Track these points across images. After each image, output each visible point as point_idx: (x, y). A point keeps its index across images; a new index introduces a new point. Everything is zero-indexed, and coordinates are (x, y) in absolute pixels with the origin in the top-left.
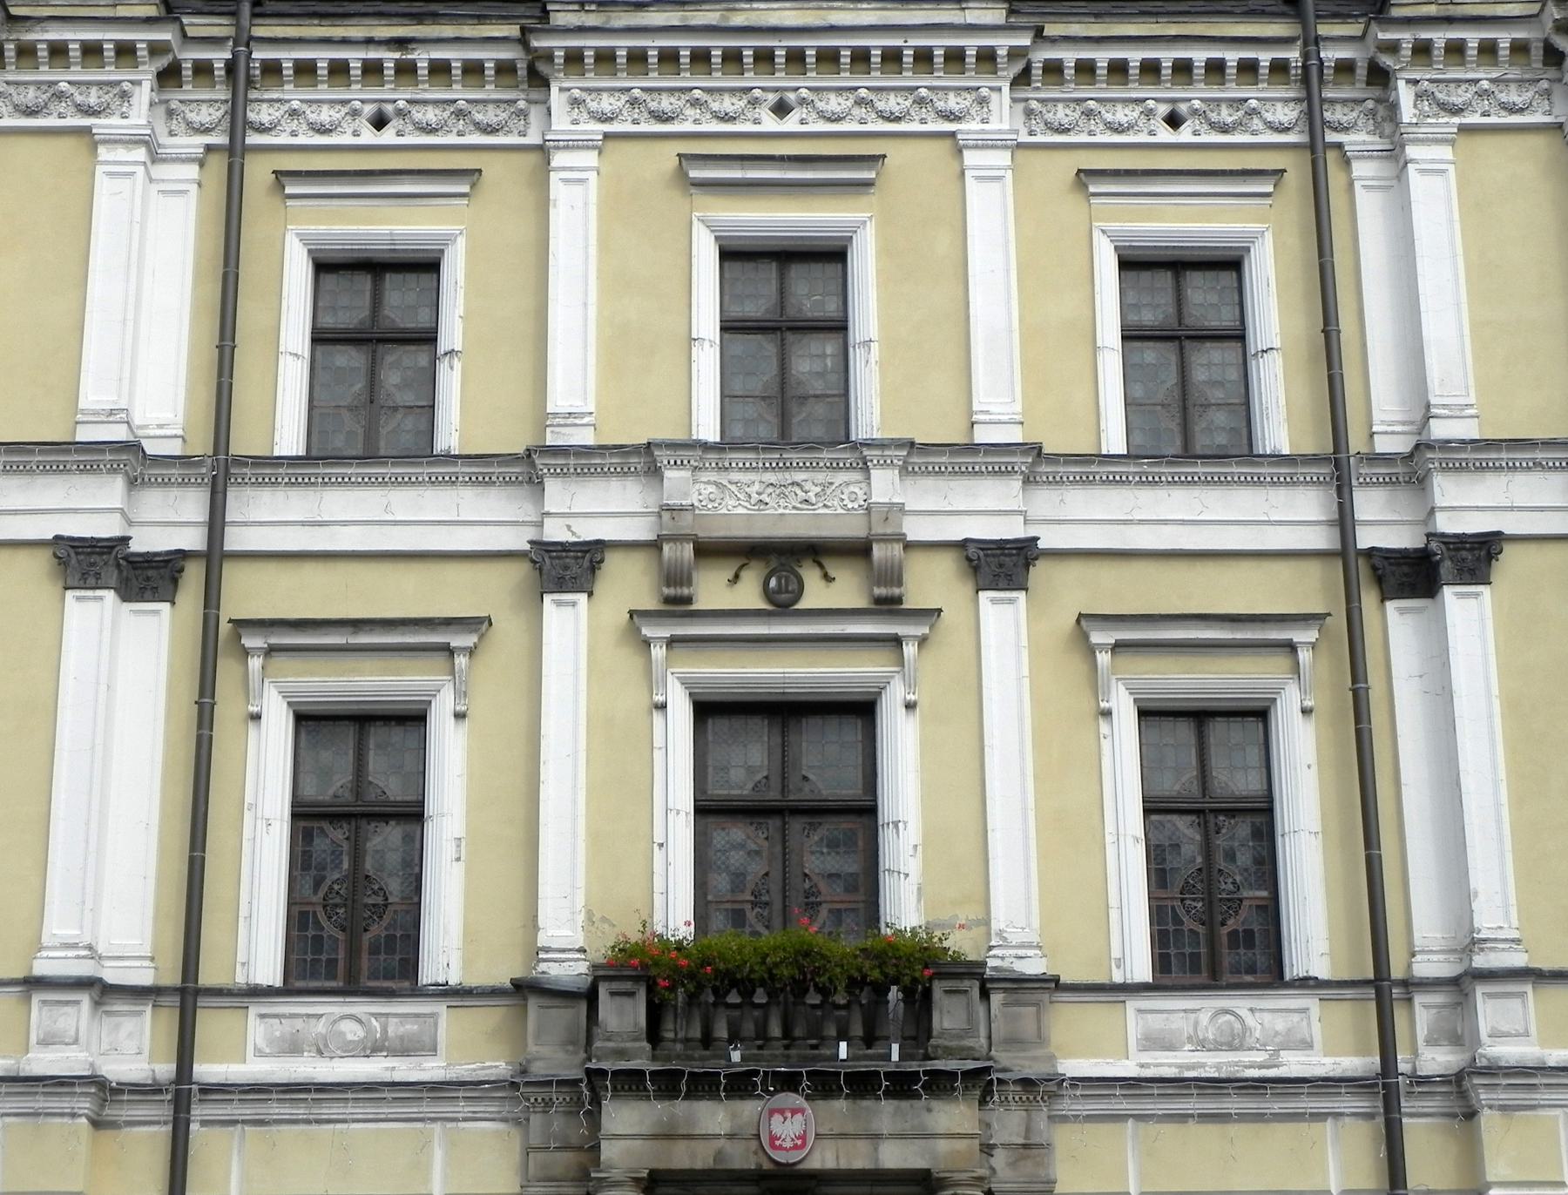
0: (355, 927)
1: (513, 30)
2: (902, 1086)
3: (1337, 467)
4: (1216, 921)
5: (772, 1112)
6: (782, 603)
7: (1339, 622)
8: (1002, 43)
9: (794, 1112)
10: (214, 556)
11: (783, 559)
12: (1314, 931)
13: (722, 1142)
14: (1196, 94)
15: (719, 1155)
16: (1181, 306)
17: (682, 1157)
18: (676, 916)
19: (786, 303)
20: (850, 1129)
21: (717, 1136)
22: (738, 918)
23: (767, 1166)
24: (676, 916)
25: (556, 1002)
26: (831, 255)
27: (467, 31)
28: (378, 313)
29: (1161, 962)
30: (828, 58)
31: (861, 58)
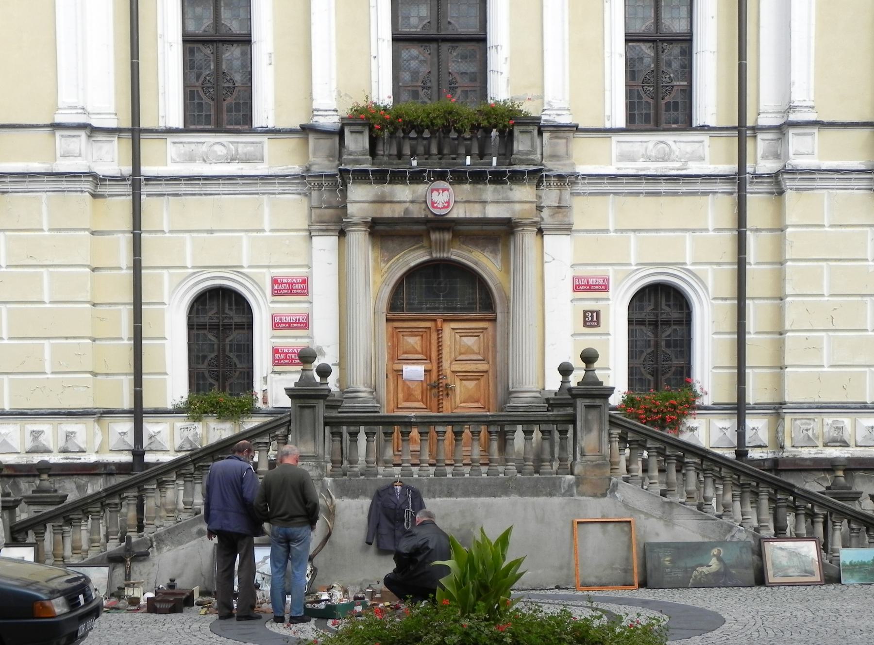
2: (498, 178)
4: (659, 94)
5: (432, 191)
9: (444, 190)
12: (710, 100)
13: (407, 205)
15: (406, 211)
17: (387, 212)
18: (383, 94)
20: (472, 198)
21: (405, 202)
22: (415, 95)
23: (430, 216)
24: (383, 94)
25: (323, 136)
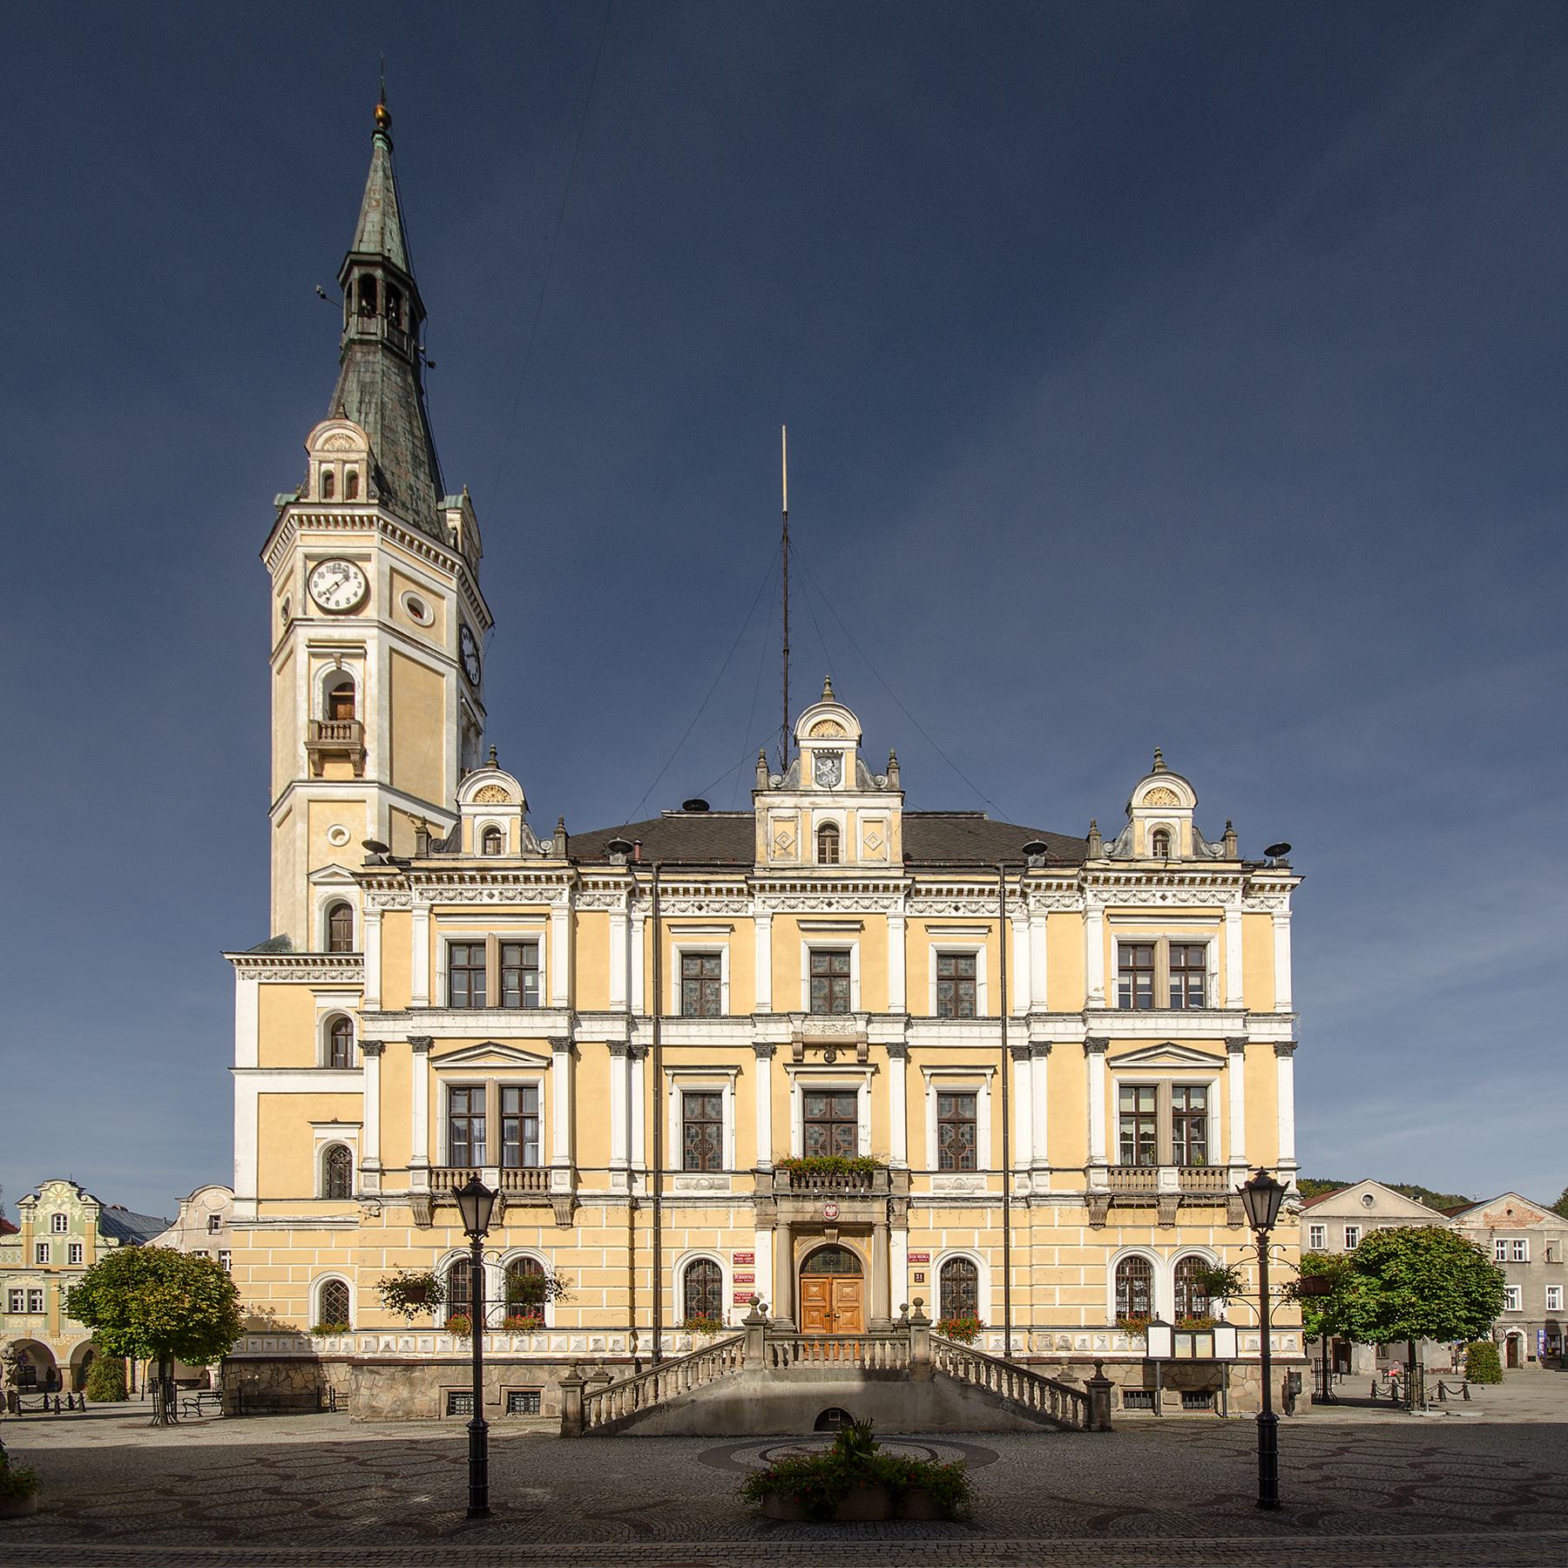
0: (702, 1150)
1: (742, 878)
3: (1003, 1020)
4: (957, 1150)
6: (830, 1062)
7: (999, 1069)
8: (902, 883)
10: (658, 1047)
11: (831, 1048)
12: (987, 1155)
14: (964, 899)
16: (956, 972)
17: (799, 1218)
18: (796, 1152)
19: (829, 971)
22: (816, 1152)
24: (796, 1152)
26: (845, 953)
27: (727, 878)
28: (701, 970)
29: (941, 1165)
30: (845, 888)
31: (856, 888)
